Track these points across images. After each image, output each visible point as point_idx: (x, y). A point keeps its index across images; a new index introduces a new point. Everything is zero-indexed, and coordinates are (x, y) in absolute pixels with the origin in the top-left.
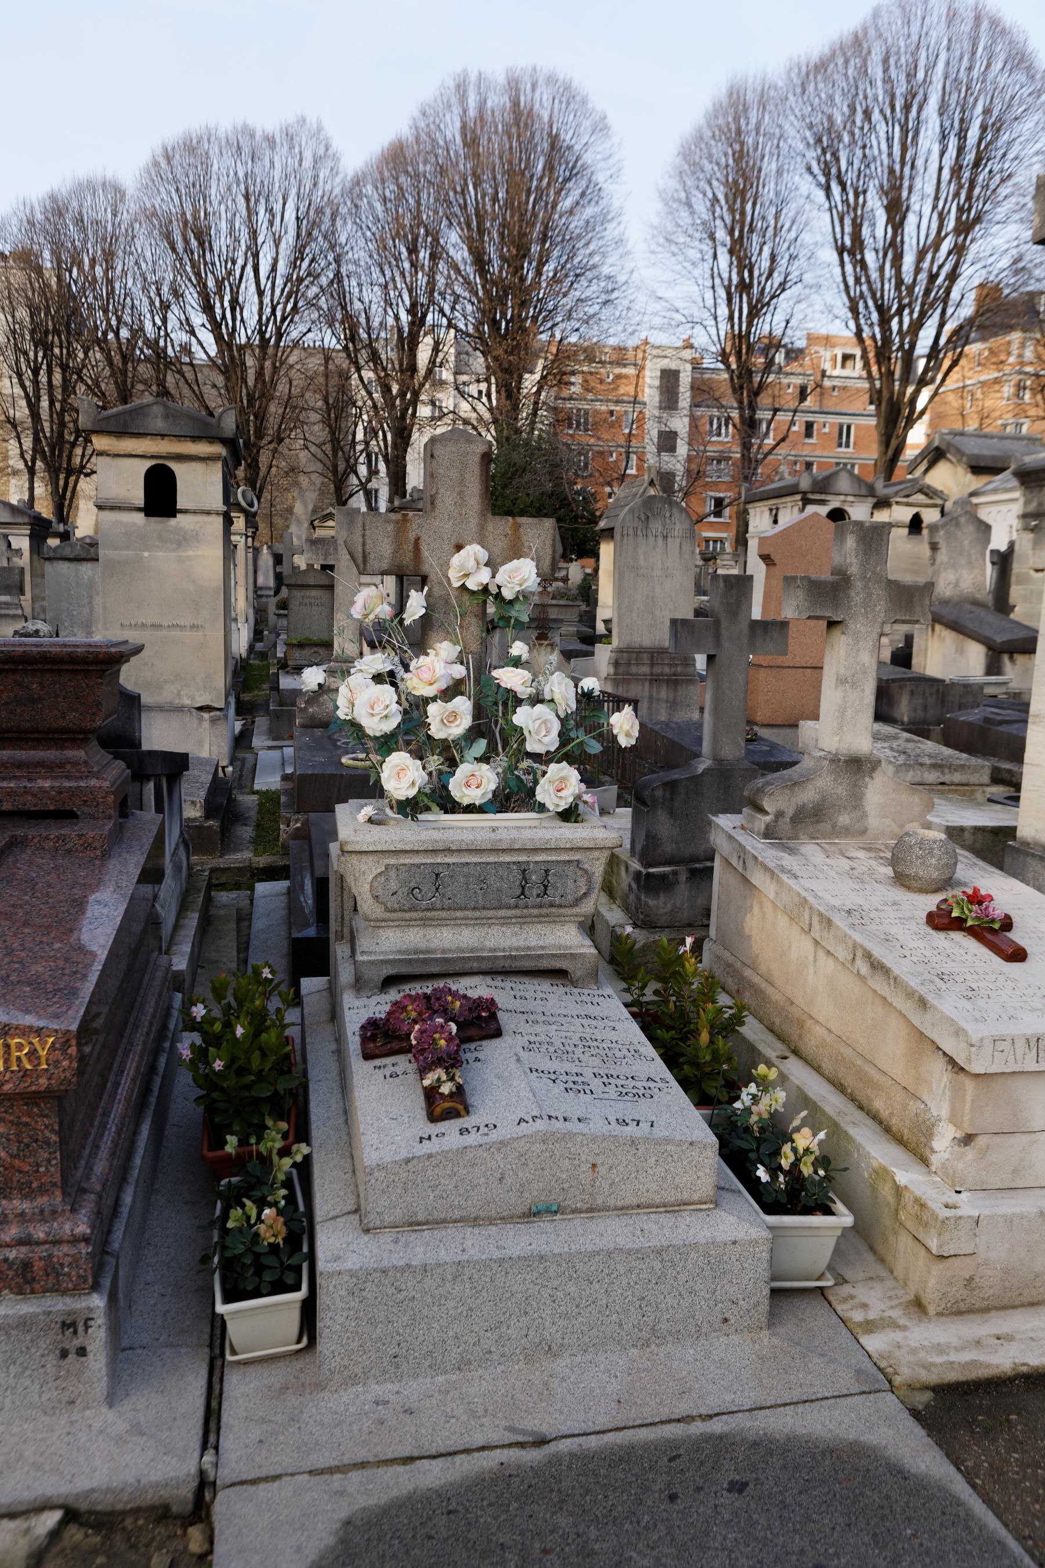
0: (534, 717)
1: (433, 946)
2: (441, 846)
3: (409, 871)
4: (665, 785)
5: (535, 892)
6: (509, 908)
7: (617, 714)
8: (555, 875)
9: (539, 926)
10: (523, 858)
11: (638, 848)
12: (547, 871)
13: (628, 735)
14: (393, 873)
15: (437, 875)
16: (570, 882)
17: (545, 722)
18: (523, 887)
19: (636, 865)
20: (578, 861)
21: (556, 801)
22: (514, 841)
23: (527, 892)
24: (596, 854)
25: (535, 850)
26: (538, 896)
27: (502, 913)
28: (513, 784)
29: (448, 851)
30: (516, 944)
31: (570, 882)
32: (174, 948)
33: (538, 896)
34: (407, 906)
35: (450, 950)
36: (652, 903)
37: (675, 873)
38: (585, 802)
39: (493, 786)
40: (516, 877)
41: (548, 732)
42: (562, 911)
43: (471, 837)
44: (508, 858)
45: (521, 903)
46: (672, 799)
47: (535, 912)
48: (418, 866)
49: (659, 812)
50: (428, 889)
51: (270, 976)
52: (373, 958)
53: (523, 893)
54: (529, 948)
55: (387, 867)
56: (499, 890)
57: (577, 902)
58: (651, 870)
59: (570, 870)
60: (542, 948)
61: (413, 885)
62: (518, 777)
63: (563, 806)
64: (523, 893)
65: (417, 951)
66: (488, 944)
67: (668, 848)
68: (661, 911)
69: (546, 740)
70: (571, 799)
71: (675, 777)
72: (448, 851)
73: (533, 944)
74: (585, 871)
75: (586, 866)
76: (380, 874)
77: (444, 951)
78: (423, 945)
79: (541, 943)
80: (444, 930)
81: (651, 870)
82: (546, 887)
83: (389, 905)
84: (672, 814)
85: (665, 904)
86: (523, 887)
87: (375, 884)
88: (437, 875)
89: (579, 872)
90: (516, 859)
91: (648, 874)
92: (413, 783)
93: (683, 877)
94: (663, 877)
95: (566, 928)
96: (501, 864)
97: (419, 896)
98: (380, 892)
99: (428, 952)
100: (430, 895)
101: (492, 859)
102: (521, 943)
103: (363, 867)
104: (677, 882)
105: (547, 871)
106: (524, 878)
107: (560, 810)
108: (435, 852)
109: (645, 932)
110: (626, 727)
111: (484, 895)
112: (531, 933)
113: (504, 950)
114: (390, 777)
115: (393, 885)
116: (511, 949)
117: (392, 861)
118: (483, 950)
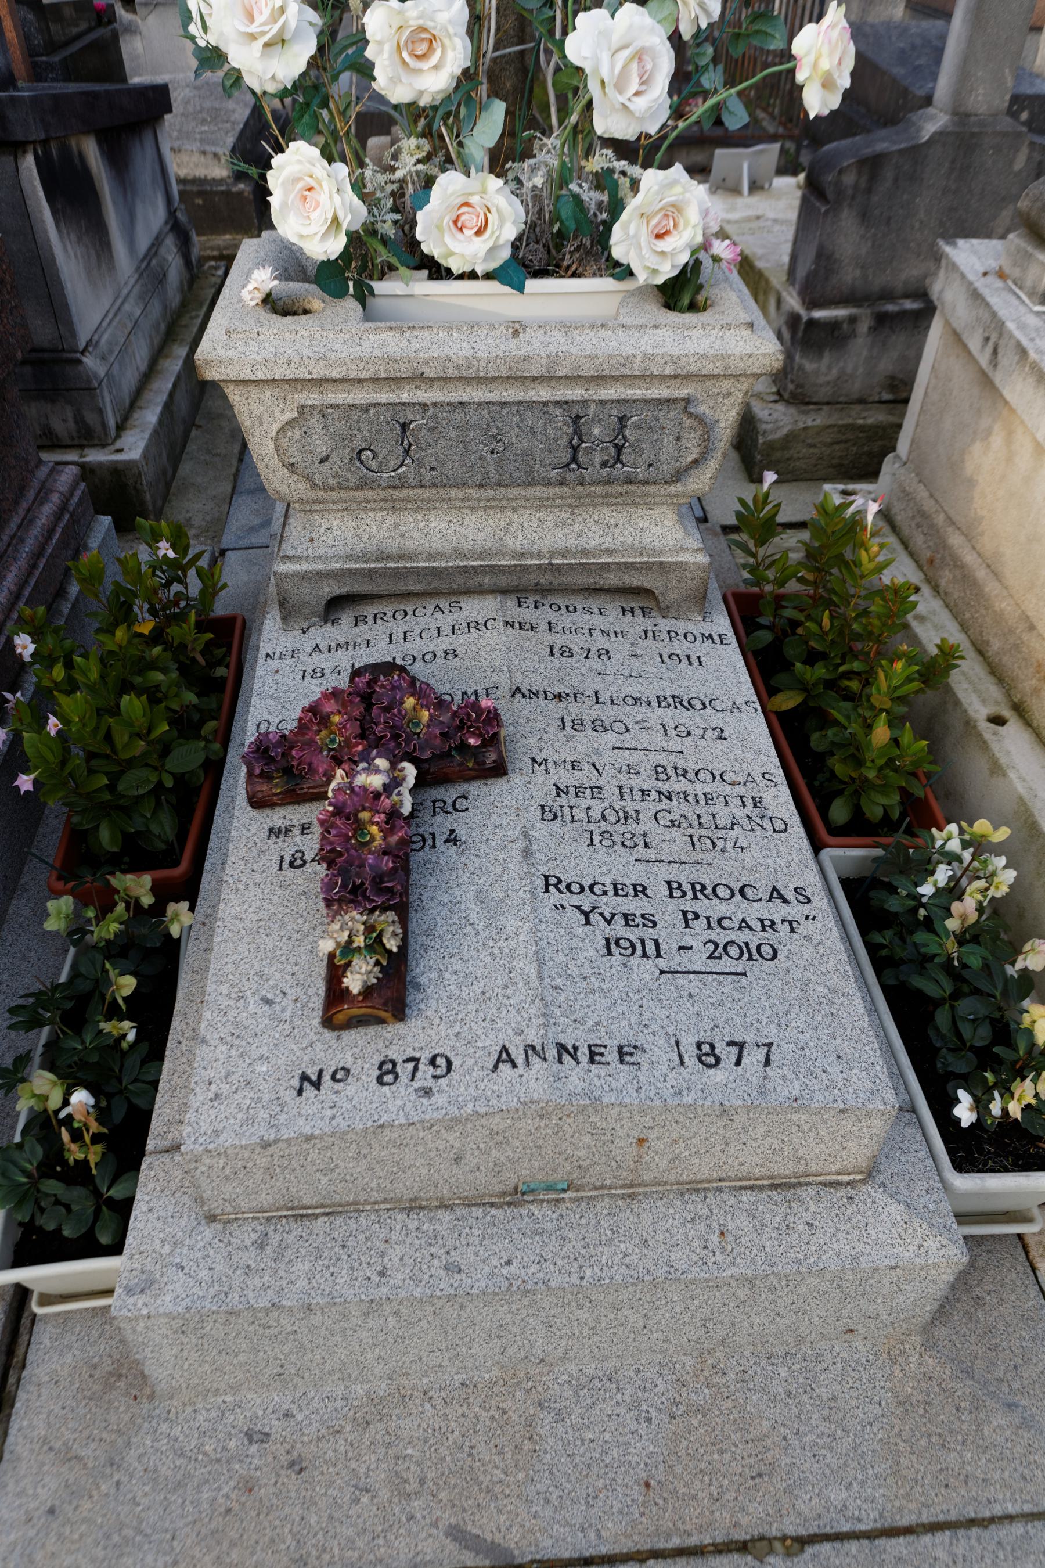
0: (616, 39)
1: (410, 545)
2: (403, 370)
3: (347, 418)
4: (862, 162)
5: (597, 458)
6: (548, 484)
7: (809, 29)
8: (638, 426)
9: (606, 510)
10: (575, 393)
11: (801, 273)
12: (622, 420)
13: (827, 84)
14: (315, 422)
15: (404, 426)
16: (668, 441)
17: (639, 56)
18: (575, 449)
19: (793, 302)
20: (687, 400)
21: (653, 262)
22: (555, 359)
23: (582, 458)
24: (726, 385)
25: (600, 379)
26: (604, 464)
27: (536, 491)
28: (566, 211)
29: (420, 379)
30: (561, 544)
31: (668, 441)
32: (136, 416)
33: (604, 464)
34: (354, 481)
35: (440, 555)
36: (809, 366)
37: (853, 320)
38: (716, 259)
39: (510, 233)
40: (560, 429)
41: (646, 81)
42: (650, 488)
43: (467, 352)
44: (544, 393)
45: (570, 476)
46: (869, 190)
47: (599, 490)
48: (365, 408)
49: (845, 213)
50: (388, 450)
51: (171, 554)
52: (303, 567)
53: (574, 459)
54: (585, 552)
55: (301, 409)
56: (528, 454)
57: (678, 476)
58: (818, 314)
59: (669, 417)
60: (609, 552)
61: (358, 443)
62: (576, 197)
63: (667, 271)
64: (574, 459)
65: (383, 556)
66: (512, 543)
67: (849, 275)
68: (822, 379)
69: (640, 104)
70: (684, 258)
71: (882, 146)
72: (420, 379)
73: (593, 544)
74: (700, 419)
75: (703, 409)
76: (290, 423)
77: (430, 557)
78: (393, 544)
79: (608, 543)
80: (432, 516)
81: (818, 314)
82: (619, 449)
83: (318, 479)
84: (864, 216)
85: (829, 368)
86: (575, 449)
87: (284, 442)
88: (404, 426)
89: (688, 422)
90: (561, 393)
91: (812, 323)
92: (336, 221)
93: (863, 327)
94: (833, 326)
95: (655, 513)
96: (530, 404)
97: (374, 464)
98: (297, 458)
99: (401, 557)
100: (393, 462)
101: (512, 394)
102: (571, 543)
103: (257, 409)
104: (853, 334)
105: (622, 420)
106: (577, 432)
107: (660, 280)
108: (394, 381)
109: (792, 410)
110: (825, 65)
111: (499, 463)
112: (591, 523)
113: (539, 556)
114: (284, 205)
115: (321, 445)
116: (552, 555)
117: (311, 398)
118: (500, 554)
